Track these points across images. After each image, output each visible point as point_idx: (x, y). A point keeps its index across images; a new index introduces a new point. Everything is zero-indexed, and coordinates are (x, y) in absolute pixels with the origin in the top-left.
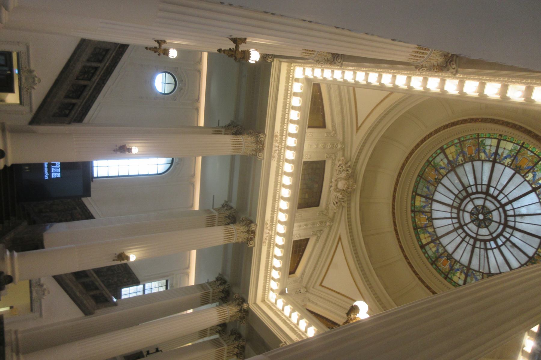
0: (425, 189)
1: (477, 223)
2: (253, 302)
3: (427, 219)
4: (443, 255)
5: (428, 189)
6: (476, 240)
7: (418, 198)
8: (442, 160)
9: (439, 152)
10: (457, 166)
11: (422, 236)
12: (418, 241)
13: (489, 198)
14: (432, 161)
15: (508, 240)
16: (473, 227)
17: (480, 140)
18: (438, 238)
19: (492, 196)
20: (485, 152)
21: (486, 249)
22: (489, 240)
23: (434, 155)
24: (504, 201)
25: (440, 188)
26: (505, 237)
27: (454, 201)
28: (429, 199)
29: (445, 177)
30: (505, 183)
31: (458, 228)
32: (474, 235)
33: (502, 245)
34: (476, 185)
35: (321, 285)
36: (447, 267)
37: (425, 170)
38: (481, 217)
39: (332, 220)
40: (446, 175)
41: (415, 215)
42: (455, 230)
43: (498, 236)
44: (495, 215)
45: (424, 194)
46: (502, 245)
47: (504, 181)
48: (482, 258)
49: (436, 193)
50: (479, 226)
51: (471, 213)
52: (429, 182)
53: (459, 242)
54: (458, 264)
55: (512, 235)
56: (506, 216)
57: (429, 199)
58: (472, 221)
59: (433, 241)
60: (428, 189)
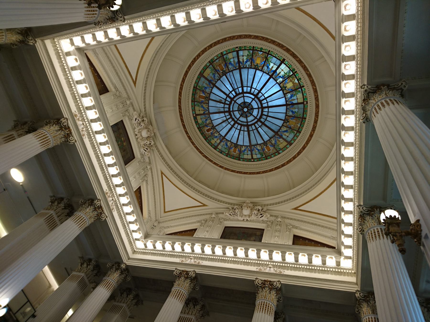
0: (296, 110)
1: (247, 104)
5: (292, 112)
7: (301, 100)
8: (288, 136)
9: (293, 141)
13: (245, 124)
14: (297, 133)
15: (225, 104)
16: (248, 100)
17: (264, 156)
18: (271, 77)
19: (244, 126)
21: (234, 90)
22: (235, 97)
23: (295, 138)
24: (236, 125)
25: (282, 116)
26: (227, 104)
27: (268, 112)
28: (289, 105)
29: (281, 126)
30: (240, 136)
31: (258, 94)
32: (245, 95)
33: (232, 91)
34: (257, 129)
37: (301, 125)
38: (245, 110)
40: (281, 127)
42: (260, 91)
43: (231, 102)
44: (237, 115)
45: (295, 106)
46: (226, 98)
47: (241, 137)
48: (234, 82)
49: (285, 111)
50: (244, 103)
51: (253, 109)
52: (295, 117)
53: (254, 84)
56: (231, 117)
57: (289, 105)
60: (292, 112)
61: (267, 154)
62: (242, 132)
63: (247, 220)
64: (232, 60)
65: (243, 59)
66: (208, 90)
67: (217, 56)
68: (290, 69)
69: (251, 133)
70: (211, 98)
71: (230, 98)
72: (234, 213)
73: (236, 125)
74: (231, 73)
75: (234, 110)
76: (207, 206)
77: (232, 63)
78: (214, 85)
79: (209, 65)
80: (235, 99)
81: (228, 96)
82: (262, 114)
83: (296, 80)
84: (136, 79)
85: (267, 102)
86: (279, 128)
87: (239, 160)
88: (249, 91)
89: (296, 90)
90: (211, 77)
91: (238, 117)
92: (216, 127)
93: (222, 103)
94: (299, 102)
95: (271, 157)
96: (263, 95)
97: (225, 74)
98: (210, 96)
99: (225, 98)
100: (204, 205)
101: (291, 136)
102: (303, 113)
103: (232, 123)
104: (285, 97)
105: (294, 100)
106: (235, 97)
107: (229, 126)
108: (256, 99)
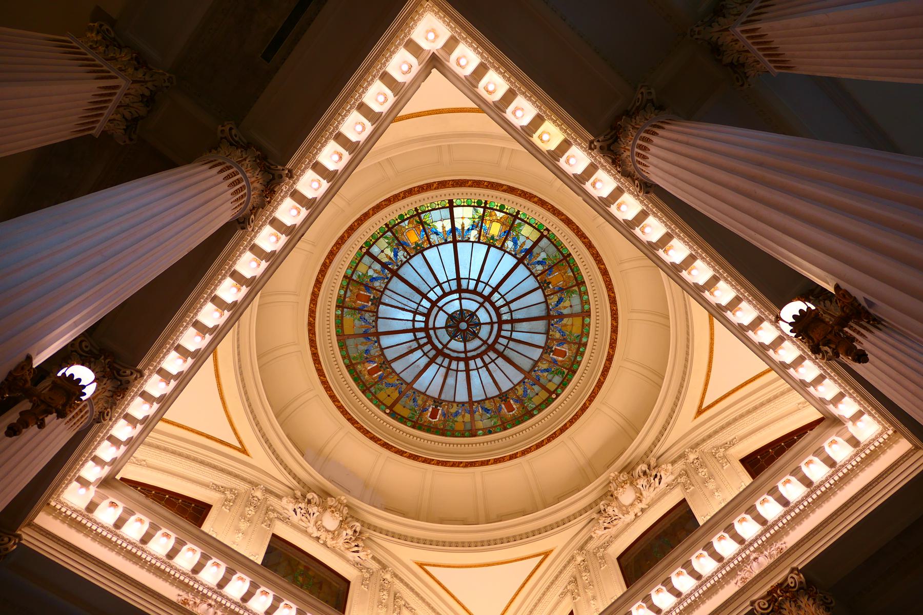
0: (543, 255)
5: (539, 263)
7: (535, 235)
9: (586, 307)
10: (549, 325)
13: (483, 348)
14: (579, 289)
15: (420, 347)
16: (454, 307)
17: (566, 371)
18: (455, 242)
20: (547, 370)
21: (415, 313)
22: (426, 322)
24: (472, 364)
25: (531, 283)
26: (425, 344)
28: (524, 257)
29: (543, 299)
32: (440, 304)
34: (510, 339)
38: (463, 326)
40: (546, 302)
42: (458, 279)
43: (428, 336)
44: (457, 345)
45: (535, 250)
46: (415, 336)
48: (405, 301)
50: (451, 317)
51: (473, 314)
55: (425, 354)
56: (452, 359)
57: (524, 257)
58: (461, 310)
60: (539, 263)
61: (568, 365)
62: (492, 366)
63: (643, 510)
64: (371, 273)
65: (387, 255)
66: (375, 352)
67: (342, 287)
68: (474, 206)
69: (508, 353)
70: (389, 359)
71: (420, 330)
72: (608, 520)
73: (472, 363)
74: (387, 292)
75: (445, 343)
76: (551, 551)
77: (375, 275)
78: (378, 334)
79: (342, 311)
80: (431, 325)
81: (414, 330)
82: (497, 309)
83: (498, 213)
84: (240, 442)
85: (487, 284)
86: (544, 305)
87: (532, 416)
88: (440, 293)
89: (512, 227)
90: (362, 327)
91: (462, 349)
92: (443, 397)
93: (415, 349)
94: (535, 240)
95: (579, 363)
96: (469, 279)
97: (378, 302)
98: (385, 357)
99: (413, 338)
100: (546, 554)
101: (575, 300)
102: (559, 250)
103: (462, 365)
104: (505, 252)
105: (524, 243)
106: (426, 322)
107: (462, 376)
108: (464, 295)
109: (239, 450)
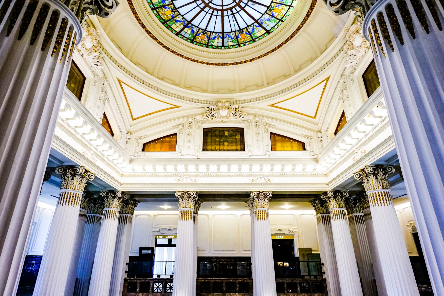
2: (119, 185)
3: (172, 11)
4: (199, 33)
6: (222, 10)
11: (173, 26)
12: (172, 31)
32: (221, 8)
35: (133, 119)
36: (206, 39)
39: (105, 78)
41: (157, 12)
54: (214, 34)
59: (185, 26)
66: (266, 17)
74: (233, 30)
77: (230, 39)
83: (162, 16)
109: (327, 81)
